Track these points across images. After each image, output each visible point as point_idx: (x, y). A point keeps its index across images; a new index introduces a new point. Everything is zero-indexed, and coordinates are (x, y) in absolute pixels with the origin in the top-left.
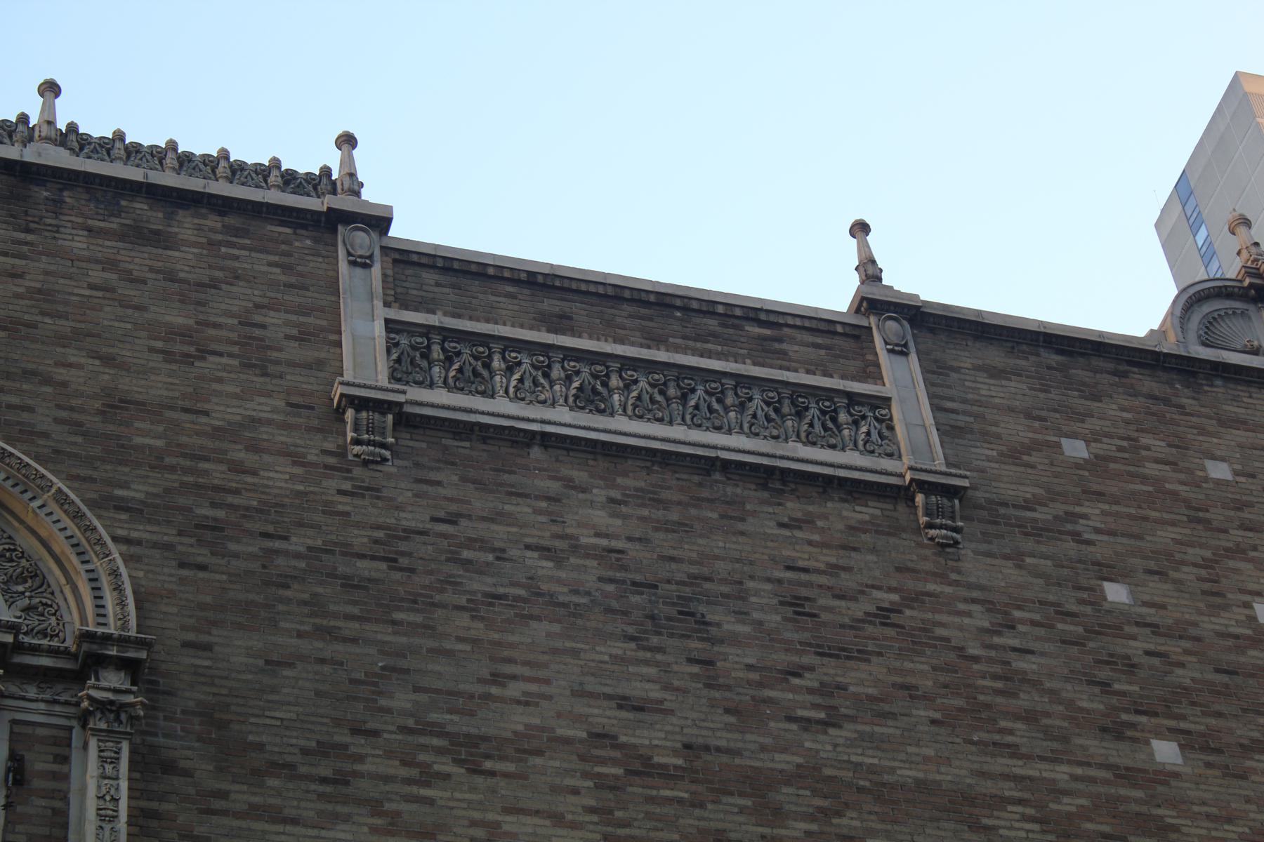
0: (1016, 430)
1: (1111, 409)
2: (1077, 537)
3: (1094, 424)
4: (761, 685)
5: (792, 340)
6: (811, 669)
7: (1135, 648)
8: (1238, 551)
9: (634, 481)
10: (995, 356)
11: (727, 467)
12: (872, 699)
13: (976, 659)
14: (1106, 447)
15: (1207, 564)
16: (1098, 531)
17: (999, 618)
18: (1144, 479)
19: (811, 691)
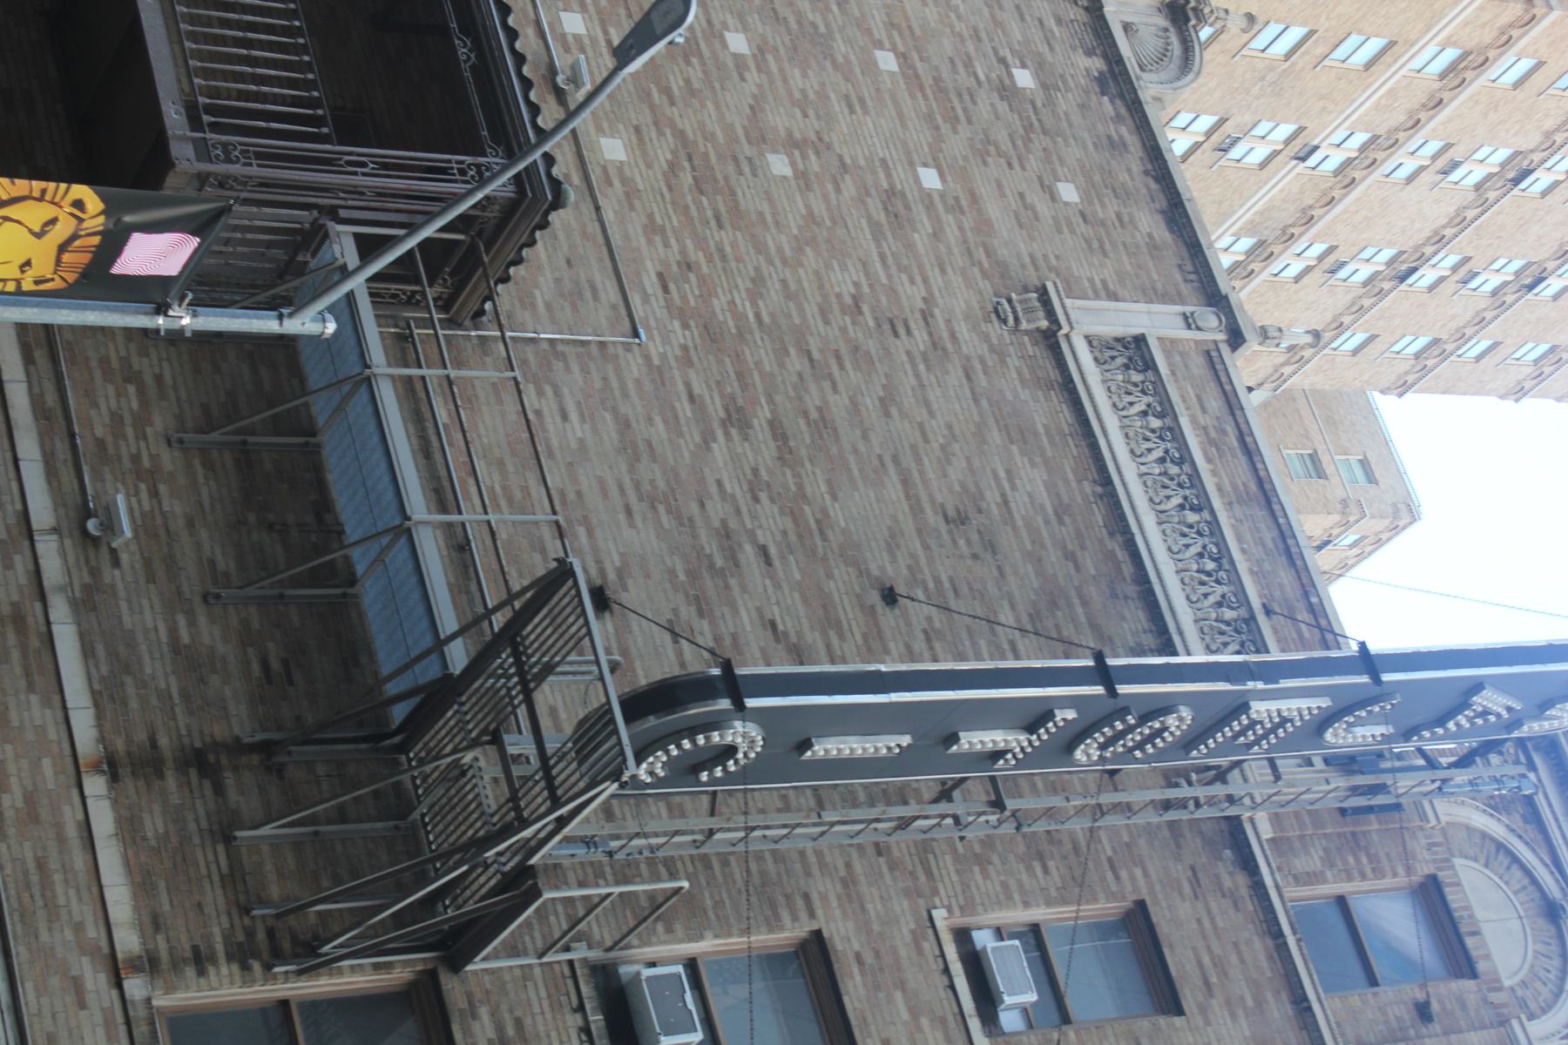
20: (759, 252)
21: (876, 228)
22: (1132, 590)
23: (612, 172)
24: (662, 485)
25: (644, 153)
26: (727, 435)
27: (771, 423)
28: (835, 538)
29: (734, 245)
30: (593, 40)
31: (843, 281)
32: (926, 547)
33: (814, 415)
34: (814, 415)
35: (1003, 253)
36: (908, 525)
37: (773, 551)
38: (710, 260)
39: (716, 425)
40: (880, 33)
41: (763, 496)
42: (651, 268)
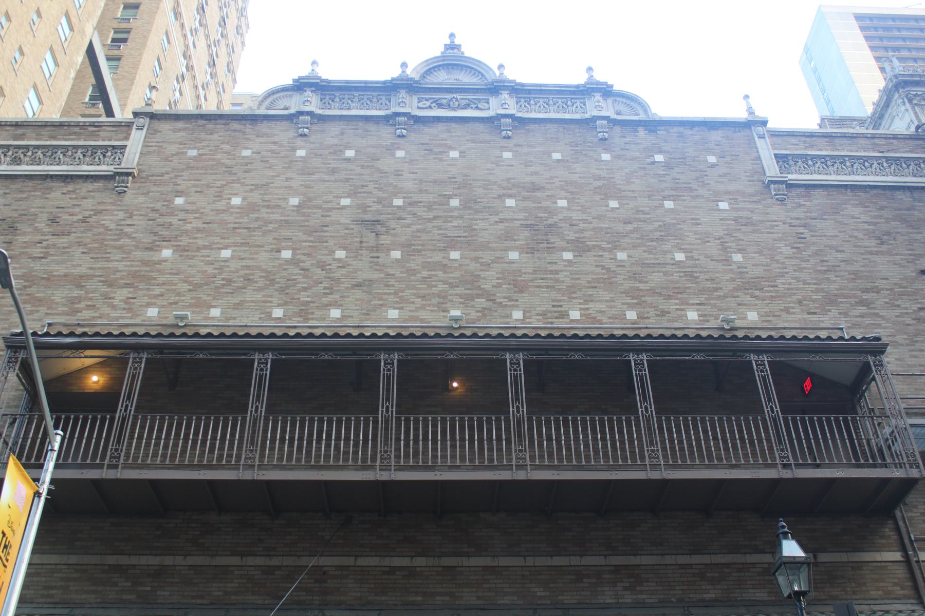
0: (172, 149)
1: (215, 136)
2: (175, 184)
3: (204, 144)
4: (25, 248)
5: (105, 131)
6: (47, 240)
7: (174, 220)
8: (238, 181)
9: (17, 185)
10: (180, 125)
11: (52, 177)
12: (64, 248)
13: (111, 230)
14: (206, 151)
15: (222, 186)
16: (184, 180)
17: (128, 215)
18: (214, 160)
19: (42, 248)
20: (783, 276)
21: (754, 232)
22: (888, 193)
23: (764, 319)
24: (905, 336)
25: (750, 305)
26: (874, 308)
27: (863, 292)
28: (904, 283)
29: (783, 284)
30: (698, 310)
31: (787, 251)
32: (897, 254)
33: (853, 276)
34: (853, 276)
35: (750, 190)
36: (891, 258)
37: (919, 306)
38: (795, 294)
39: (871, 311)
40: (657, 203)
41: (897, 303)
42: (806, 316)
